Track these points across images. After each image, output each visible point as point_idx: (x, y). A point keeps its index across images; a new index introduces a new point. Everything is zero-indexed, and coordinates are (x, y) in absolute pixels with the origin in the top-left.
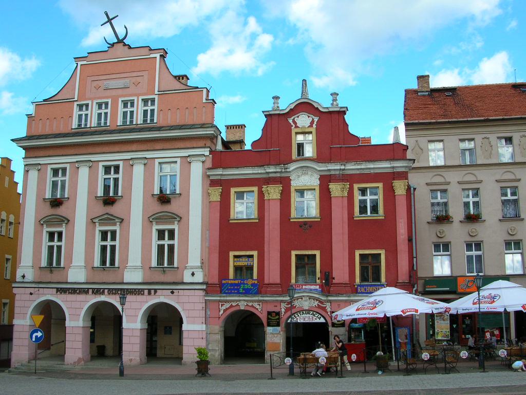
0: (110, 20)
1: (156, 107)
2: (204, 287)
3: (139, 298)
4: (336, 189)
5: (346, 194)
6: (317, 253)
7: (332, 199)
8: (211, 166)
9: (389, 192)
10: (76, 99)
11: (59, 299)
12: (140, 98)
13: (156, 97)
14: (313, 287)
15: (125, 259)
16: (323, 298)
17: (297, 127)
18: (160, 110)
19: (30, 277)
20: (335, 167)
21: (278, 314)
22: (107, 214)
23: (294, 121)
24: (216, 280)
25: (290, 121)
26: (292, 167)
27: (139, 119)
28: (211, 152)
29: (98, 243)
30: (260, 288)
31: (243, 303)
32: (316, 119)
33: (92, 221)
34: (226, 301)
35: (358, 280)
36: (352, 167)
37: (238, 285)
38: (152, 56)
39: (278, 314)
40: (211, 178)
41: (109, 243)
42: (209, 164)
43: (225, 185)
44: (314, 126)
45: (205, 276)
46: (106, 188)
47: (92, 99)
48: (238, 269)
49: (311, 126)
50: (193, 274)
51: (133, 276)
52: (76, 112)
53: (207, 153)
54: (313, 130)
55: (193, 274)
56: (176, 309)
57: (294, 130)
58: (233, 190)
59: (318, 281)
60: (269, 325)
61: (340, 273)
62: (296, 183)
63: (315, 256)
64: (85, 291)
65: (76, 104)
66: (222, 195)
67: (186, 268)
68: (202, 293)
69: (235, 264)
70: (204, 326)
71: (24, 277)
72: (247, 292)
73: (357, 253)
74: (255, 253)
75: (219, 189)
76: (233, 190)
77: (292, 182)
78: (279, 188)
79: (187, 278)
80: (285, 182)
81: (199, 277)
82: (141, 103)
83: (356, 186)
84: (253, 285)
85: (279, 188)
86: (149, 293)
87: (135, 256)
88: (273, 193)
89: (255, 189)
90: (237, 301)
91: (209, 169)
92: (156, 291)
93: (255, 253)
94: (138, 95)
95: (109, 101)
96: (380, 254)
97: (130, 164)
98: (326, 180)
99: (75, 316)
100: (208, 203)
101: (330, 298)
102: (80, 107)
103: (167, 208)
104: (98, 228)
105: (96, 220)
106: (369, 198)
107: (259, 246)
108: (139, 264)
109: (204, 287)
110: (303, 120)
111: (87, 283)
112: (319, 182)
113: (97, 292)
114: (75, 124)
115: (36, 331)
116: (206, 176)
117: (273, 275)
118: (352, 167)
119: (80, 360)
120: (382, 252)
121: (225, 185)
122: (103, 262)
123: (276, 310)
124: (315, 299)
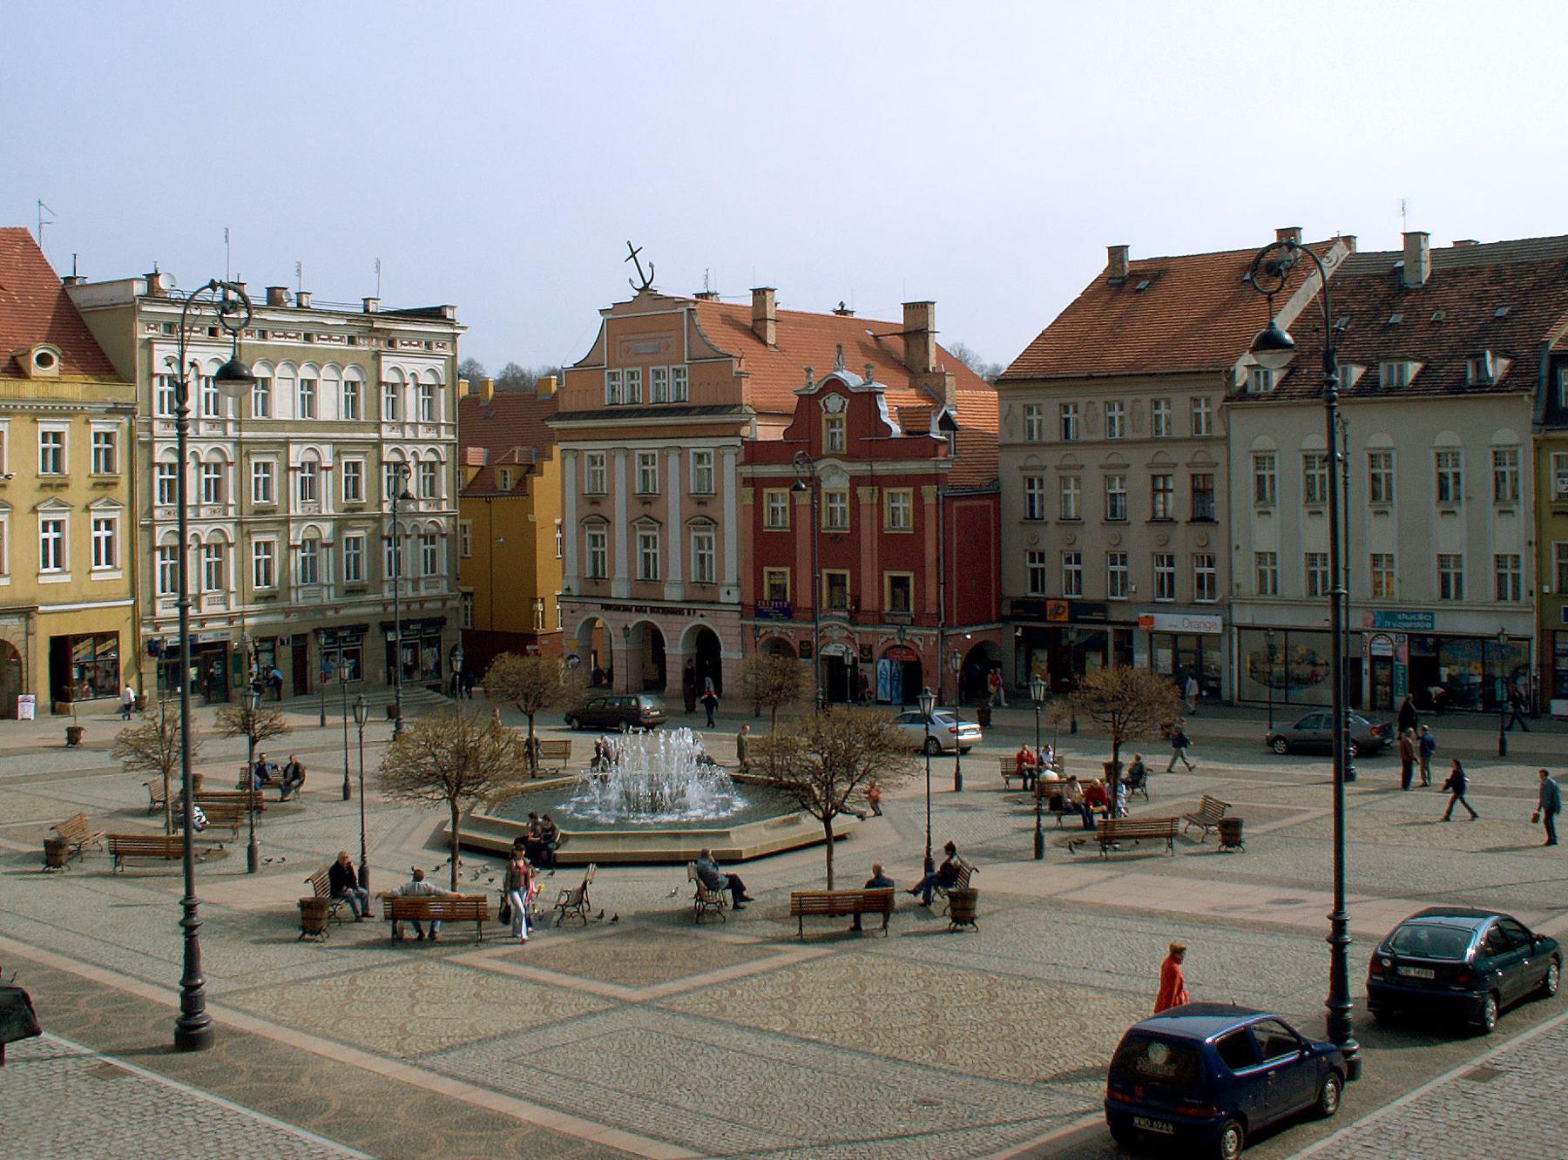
0: (633, 254)
1: (686, 379)
2: (739, 608)
3: (679, 618)
4: (863, 492)
5: (875, 501)
6: (847, 572)
7: (862, 508)
8: (743, 460)
10: (605, 366)
12: (671, 367)
14: (842, 614)
15: (665, 572)
16: (850, 628)
17: (827, 412)
18: (691, 385)
20: (861, 468)
21: (809, 643)
22: (646, 516)
24: (750, 601)
25: (821, 404)
26: (820, 465)
30: (788, 612)
35: (887, 608)
36: (881, 468)
38: (679, 310)
39: (809, 643)
40: (744, 476)
41: (650, 551)
42: (742, 458)
43: (756, 484)
45: (742, 594)
46: (646, 486)
48: (773, 587)
49: (841, 411)
50: (728, 593)
51: (673, 594)
53: (739, 444)
54: (843, 416)
55: (728, 593)
56: (714, 634)
57: (825, 417)
58: (766, 491)
59: (848, 606)
60: (801, 656)
61: (868, 602)
62: (826, 486)
63: (844, 576)
64: (627, 609)
65: (606, 372)
66: (755, 495)
67: (722, 585)
68: (737, 615)
69: (772, 582)
70: (741, 654)
73: (887, 575)
74: (787, 570)
75: (750, 491)
76: (766, 491)
77: (823, 485)
79: (723, 598)
80: (814, 482)
81: (735, 597)
83: (886, 491)
88: (804, 499)
90: (771, 627)
91: (741, 464)
92: (694, 610)
93: (787, 570)
95: (640, 369)
96: (908, 577)
98: (856, 481)
100: (741, 507)
101: (858, 629)
102: (613, 376)
103: (702, 510)
105: (634, 523)
107: (791, 561)
108: (679, 578)
109: (739, 608)
110: (834, 403)
111: (631, 599)
112: (849, 485)
113: (640, 610)
116: (738, 474)
118: (881, 468)
121: (756, 484)
122: (647, 575)
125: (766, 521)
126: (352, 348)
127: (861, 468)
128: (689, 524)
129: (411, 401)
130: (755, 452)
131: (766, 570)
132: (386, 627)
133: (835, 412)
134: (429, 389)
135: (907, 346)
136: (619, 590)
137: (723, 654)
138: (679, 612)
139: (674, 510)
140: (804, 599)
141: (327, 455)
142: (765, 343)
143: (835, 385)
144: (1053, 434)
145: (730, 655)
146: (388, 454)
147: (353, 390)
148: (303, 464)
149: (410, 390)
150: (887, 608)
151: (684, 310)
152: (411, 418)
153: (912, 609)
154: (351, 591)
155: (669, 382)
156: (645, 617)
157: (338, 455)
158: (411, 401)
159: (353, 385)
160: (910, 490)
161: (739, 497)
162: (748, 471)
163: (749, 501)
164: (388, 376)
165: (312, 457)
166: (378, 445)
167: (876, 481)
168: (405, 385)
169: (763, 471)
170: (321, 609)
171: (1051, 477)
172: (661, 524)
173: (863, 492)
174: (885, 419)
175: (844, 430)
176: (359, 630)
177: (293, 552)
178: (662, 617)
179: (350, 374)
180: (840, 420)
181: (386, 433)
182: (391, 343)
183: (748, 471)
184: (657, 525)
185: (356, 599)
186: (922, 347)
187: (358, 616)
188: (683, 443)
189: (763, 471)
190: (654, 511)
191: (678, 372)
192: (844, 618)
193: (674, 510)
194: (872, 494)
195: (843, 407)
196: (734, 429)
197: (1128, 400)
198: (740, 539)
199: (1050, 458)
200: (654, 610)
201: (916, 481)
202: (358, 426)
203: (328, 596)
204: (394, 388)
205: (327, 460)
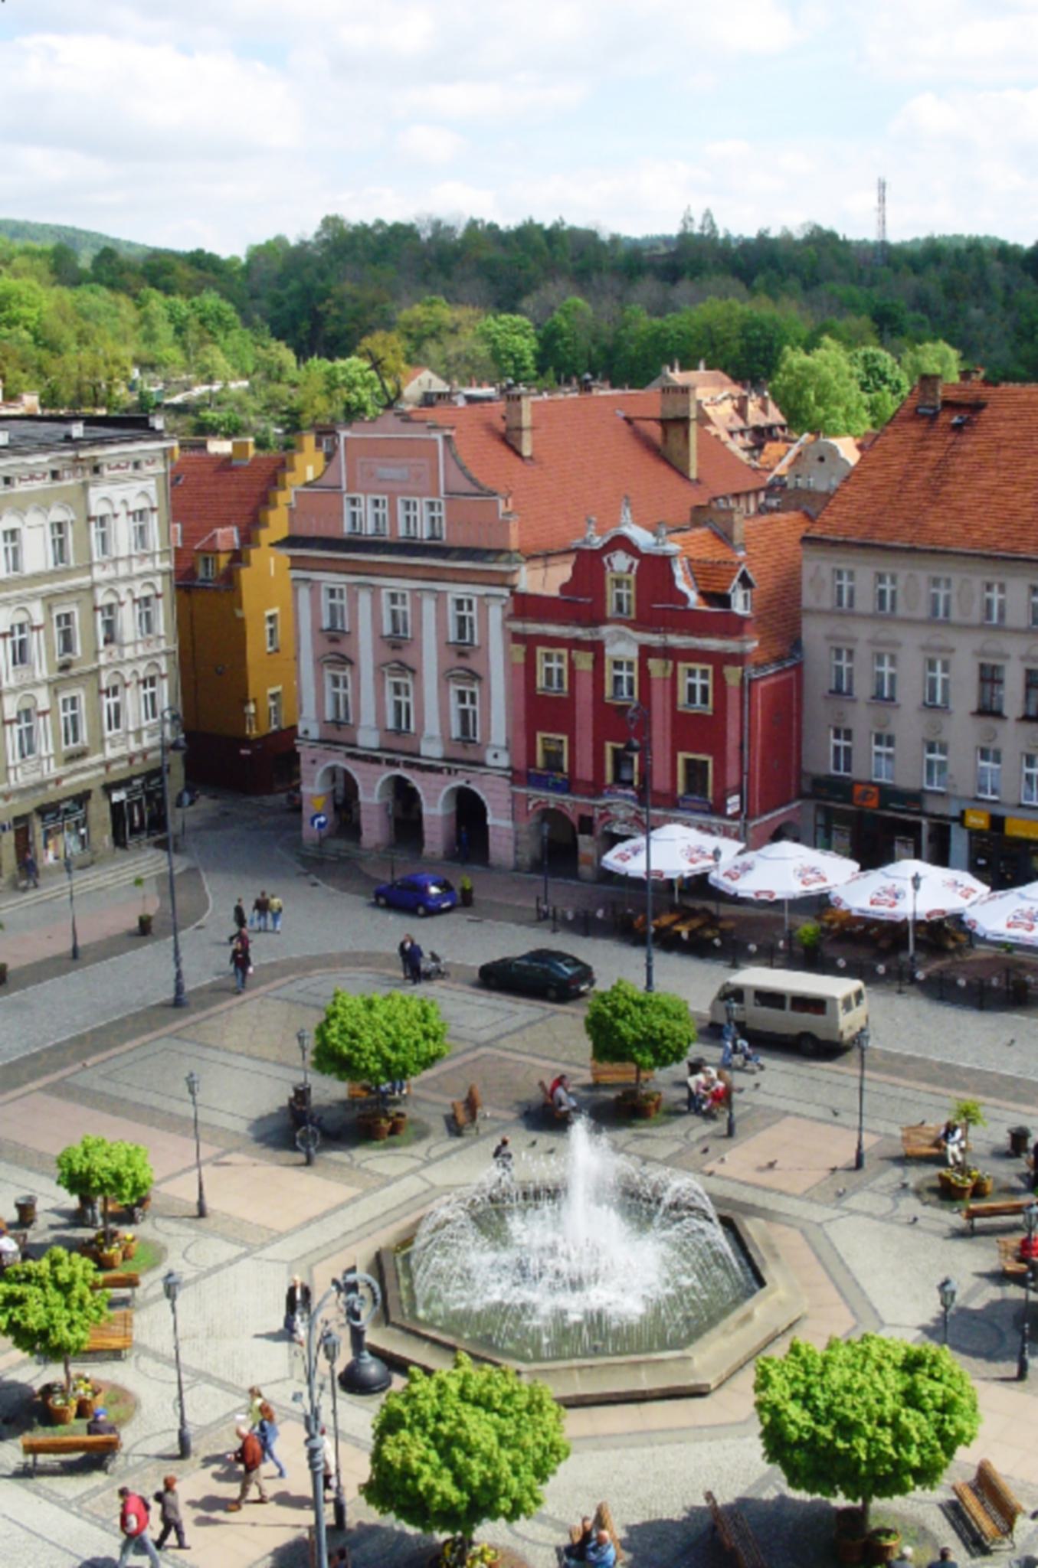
1: (443, 514)
2: (509, 774)
3: (439, 777)
4: (655, 665)
9: (720, 680)
11: (351, 767)
13: (443, 503)
15: (421, 724)
19: (314, 733)
20: (654, 639)
23: (609, 561)
24: (522, 765)
25: (605, 560)
27: (423, 532)
28: (512, 593)
29: (389, 697)
30: (569, 786)
31: (553, 799)
32: (636, 562)
33: (380, 669)
34: (537, 796)
35: (681, 790)
36: (675, 640)
37: (547, 777)
39: (591, 819)
42: (510, 609)
44: (634, 572)
45: (512, 757)
47: (366, 492)
48: (546, 752)
49: (629, 571)
50: (496, 756)
52: (347, 509)
53: (506, 592)
54: (632, 577)
55: (496, 756)
57: (609, 576)
60: (583, 832)
61: (660, 781)
62: (613, 651)
68: (507, 782)
71: (306, 732)
72: (557, 788)
73: (681, 756)
74: (565, 738)
78: (590, 656)
80: (597, 648)
81: (504, 761)
82: (425, 508)
83: (681, 666)
84: (563, 779)
85: (590, 656)
86: (449, 772)
87: (432, 725)
88: (585, 662)
89: (564, 652)
92: (456, 771)
93: (565, 738)
94: (420, 495)
95: (386, 498)
97: (417, 595)
98: (646, 652)
99: (370, 790)
100: (510, 665)
102: (353, 502)
103: (463, 662)
104: (389, 680)
105: (386, 669)
106: (698, 681)
110: (620, 562)
111: (380, 750)
113: (392, 763)
114: (347, 527)
115: (318, 816)
117: (585, 771)
118: (675, 640)
119: (377, 846)
120: (710, 759)
123: (589, 814)
124: (631, 808)
125: (541, 682)
126: (57, 484)
127: (654, 639)
128: (447, 676)
129: (123, 532)
130: (526, 606)
131: (540, 736)
132: (109, 788)
133: (621, 572)
134: (141, 514)
135: (665, 433)
136: (368, 738)
137: (490, 821)
138: (439, 770)
139: (430, 659)
140: (585, 771)
141: (37, 613)
142: (518, 454)
143: (622, 543)
144: (865, 603)
145: (498, 821)
146: (102, 598)
147: (60, 531)
148: (12, 627)
149: (123, 516)
150: (681, 790)
151: (438, 436)
152: (124, 552)
153: (710, 794)
154: (71, 758)
155: (423, 514)
156: (398, 772)
157: (49, 608)
158: (123, 532)
159: (60, 527)
160: (710, 668)
161: (508, 655)
162: (517, 626)
163: (520, 659)
164: (97, 509)
165: (22, 617)
166: (92, 588)
167: (669, 653)
168: (116, 516)
169: (534, 628)
170: (42, 785)
171: (863, 651)
172: (413, 671)
173: (655, 665)
174: (682, 585)
175: (632, 592)
176: (82, 798)
177: (8, 728)
178: (419, 775)
179: (58, 515)
180: (628, 582)
181: (99, 574)
182: (96, 470)
183: (517, 626)
184: (410, 675)
185: (79, 764)
186: (681, 435)
187: (82, 782)
188: (439, 586)
189: (534, 628)
190: (407, 656)
191: (431, 505)
192: (632, 798)
193: (430, 659)
194: (666, 668)
195: (631, 566)
196: (503, 580)
197: (956, 580)
198: (510, 695)
199: (863, 632)
200: (409, 765)
201: (719, 660)
202: (68, 573)
203: (52, 770)
204: (102, 520)
205: (39, 618)
